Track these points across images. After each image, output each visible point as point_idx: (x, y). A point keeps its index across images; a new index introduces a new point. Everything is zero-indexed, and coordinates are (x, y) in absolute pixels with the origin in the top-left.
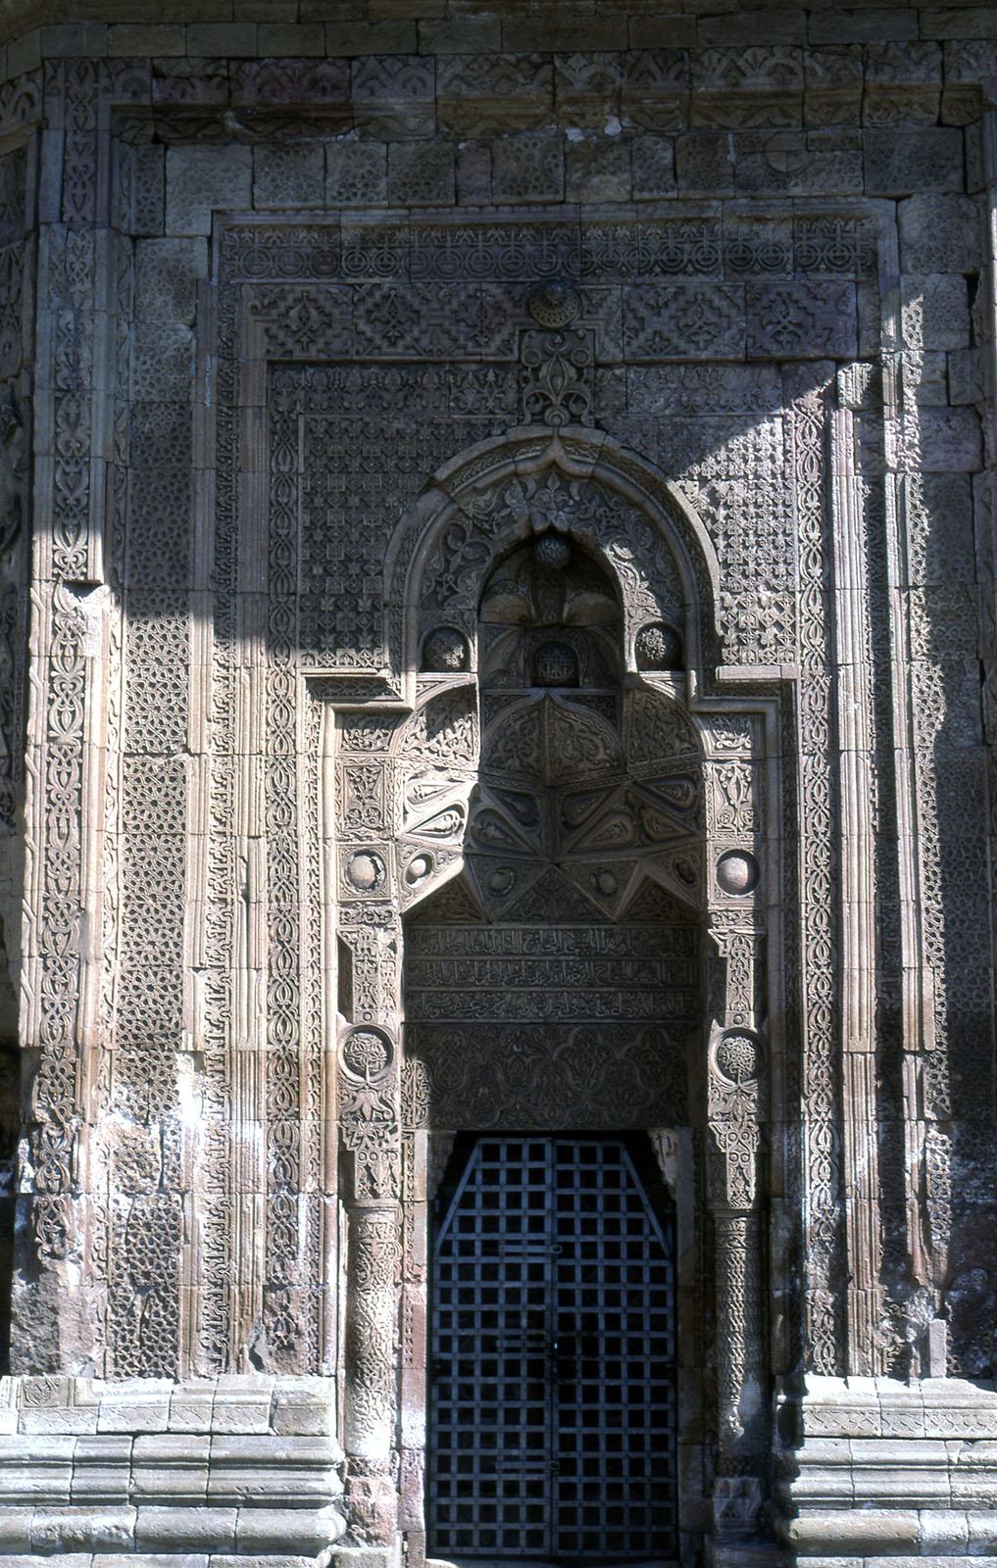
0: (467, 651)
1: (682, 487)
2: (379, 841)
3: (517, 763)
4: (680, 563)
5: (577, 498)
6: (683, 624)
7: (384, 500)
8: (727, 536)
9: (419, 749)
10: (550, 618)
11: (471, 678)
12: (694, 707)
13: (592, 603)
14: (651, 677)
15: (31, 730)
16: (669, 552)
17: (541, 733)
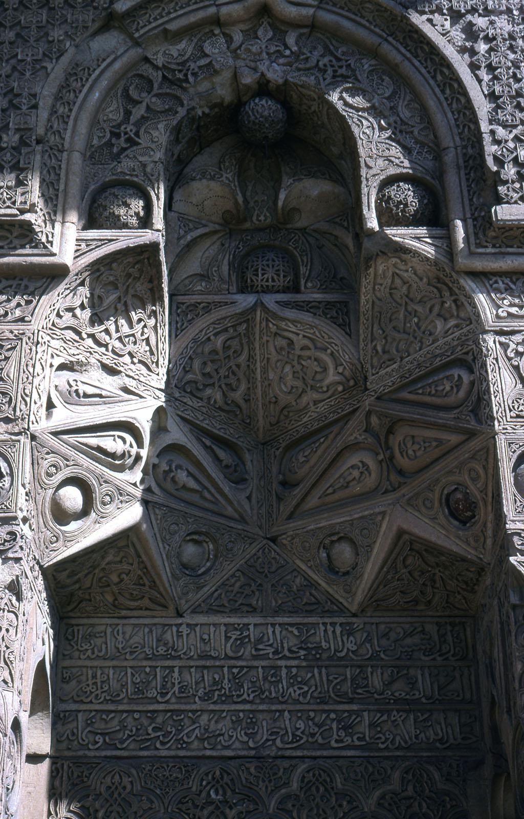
0: (148, 208)
1: (430, 21)
2: (7, 437)
3: (218, 396)
4: (431, 103)
5: (295, 49)
6: (440, 174)
7: (47, 34)
8: (491, 68)
9: (78, 333)
10: (262, 217)
11: (156, 234)
12: (463, 262)
14: (397, 234)
16: (417, 97)
17: (250, 357)
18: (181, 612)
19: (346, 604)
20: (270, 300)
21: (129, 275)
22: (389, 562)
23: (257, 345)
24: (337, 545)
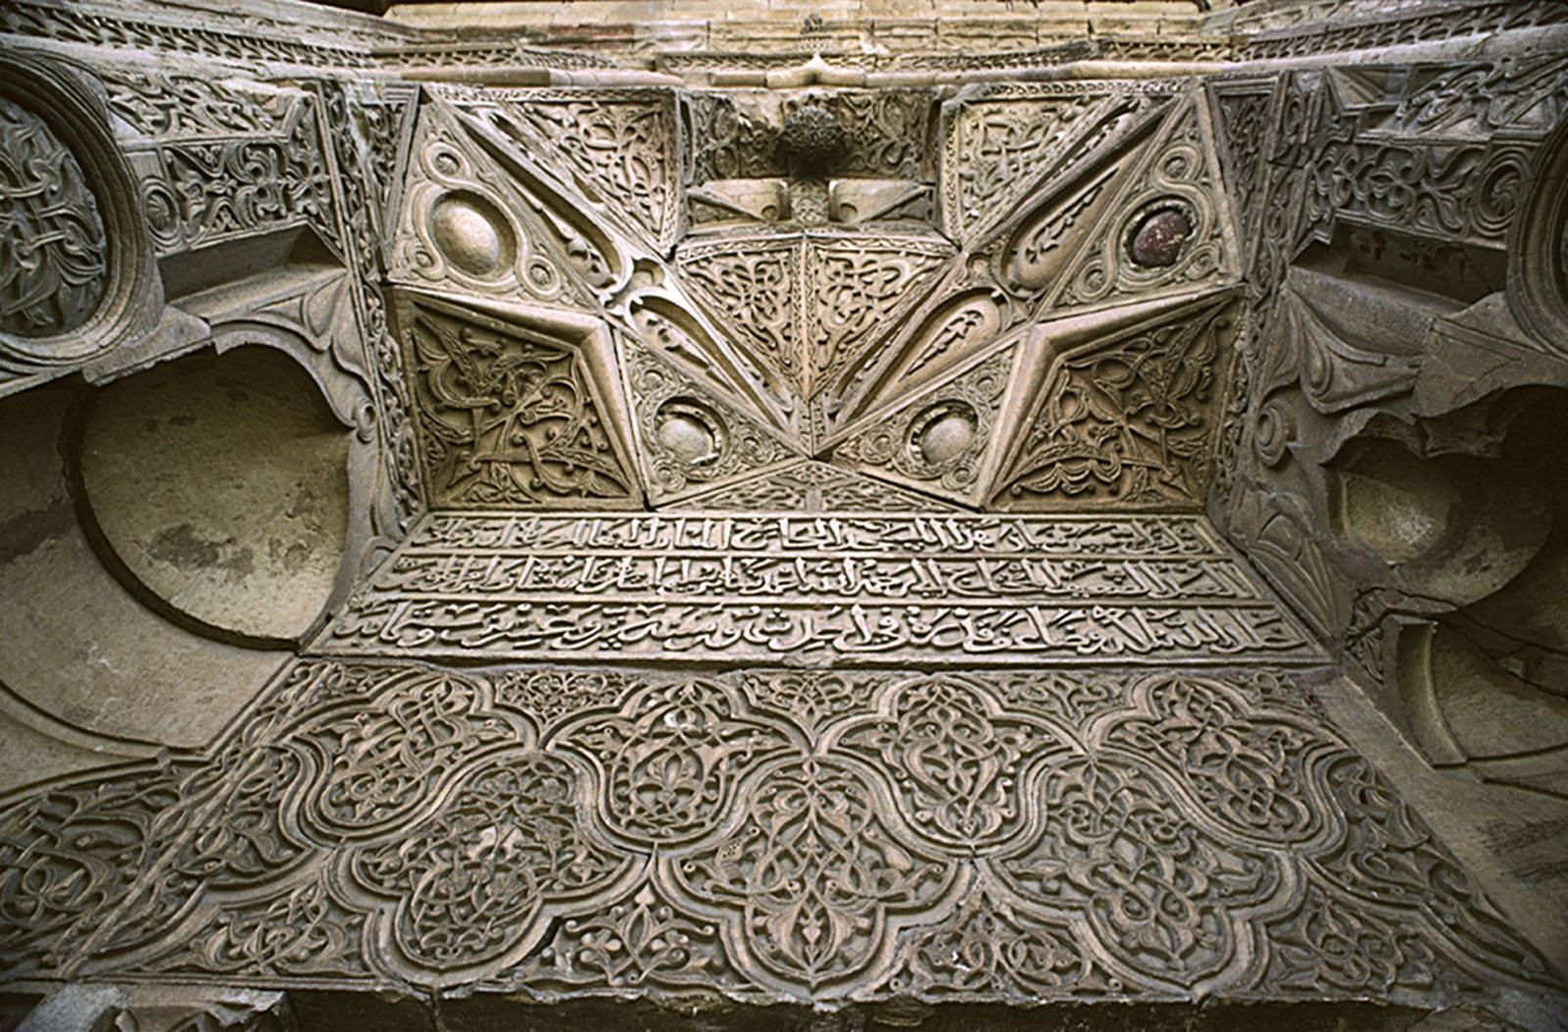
3: (746, 313)
13: (874, 191)
18: (652, 503)
19: (960, 498)
21: (630, 130)
22: (1036, 405)
23: (802, 278)
24: (936, 429)
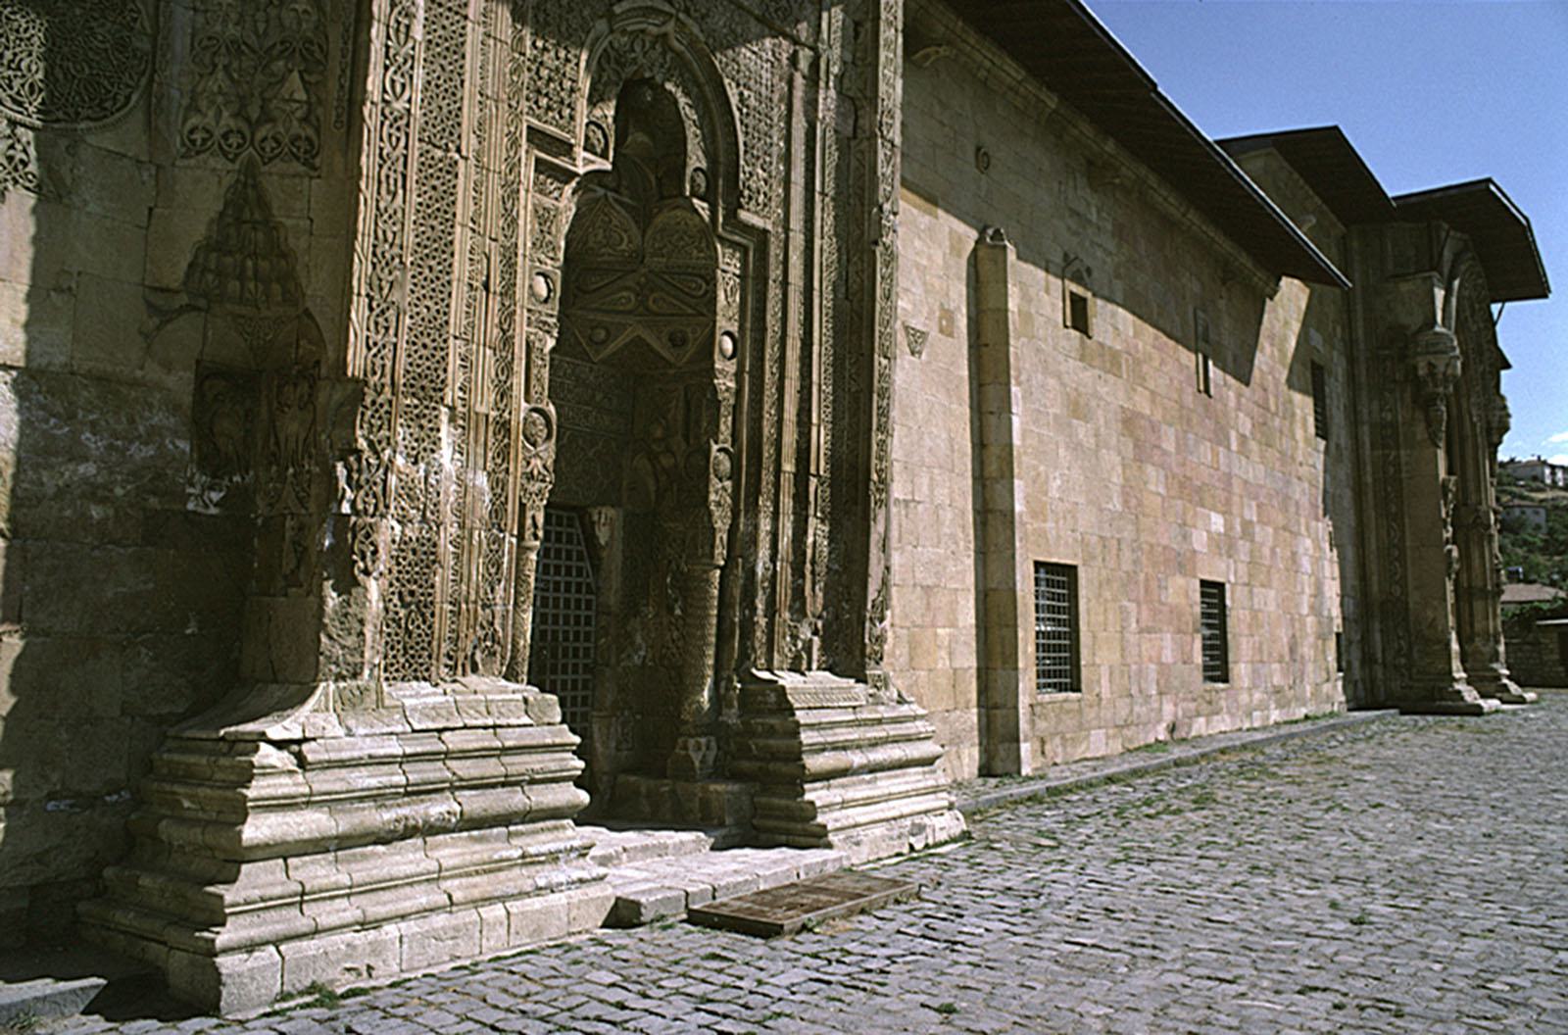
15: (370, 87)
20: (609, 194)
